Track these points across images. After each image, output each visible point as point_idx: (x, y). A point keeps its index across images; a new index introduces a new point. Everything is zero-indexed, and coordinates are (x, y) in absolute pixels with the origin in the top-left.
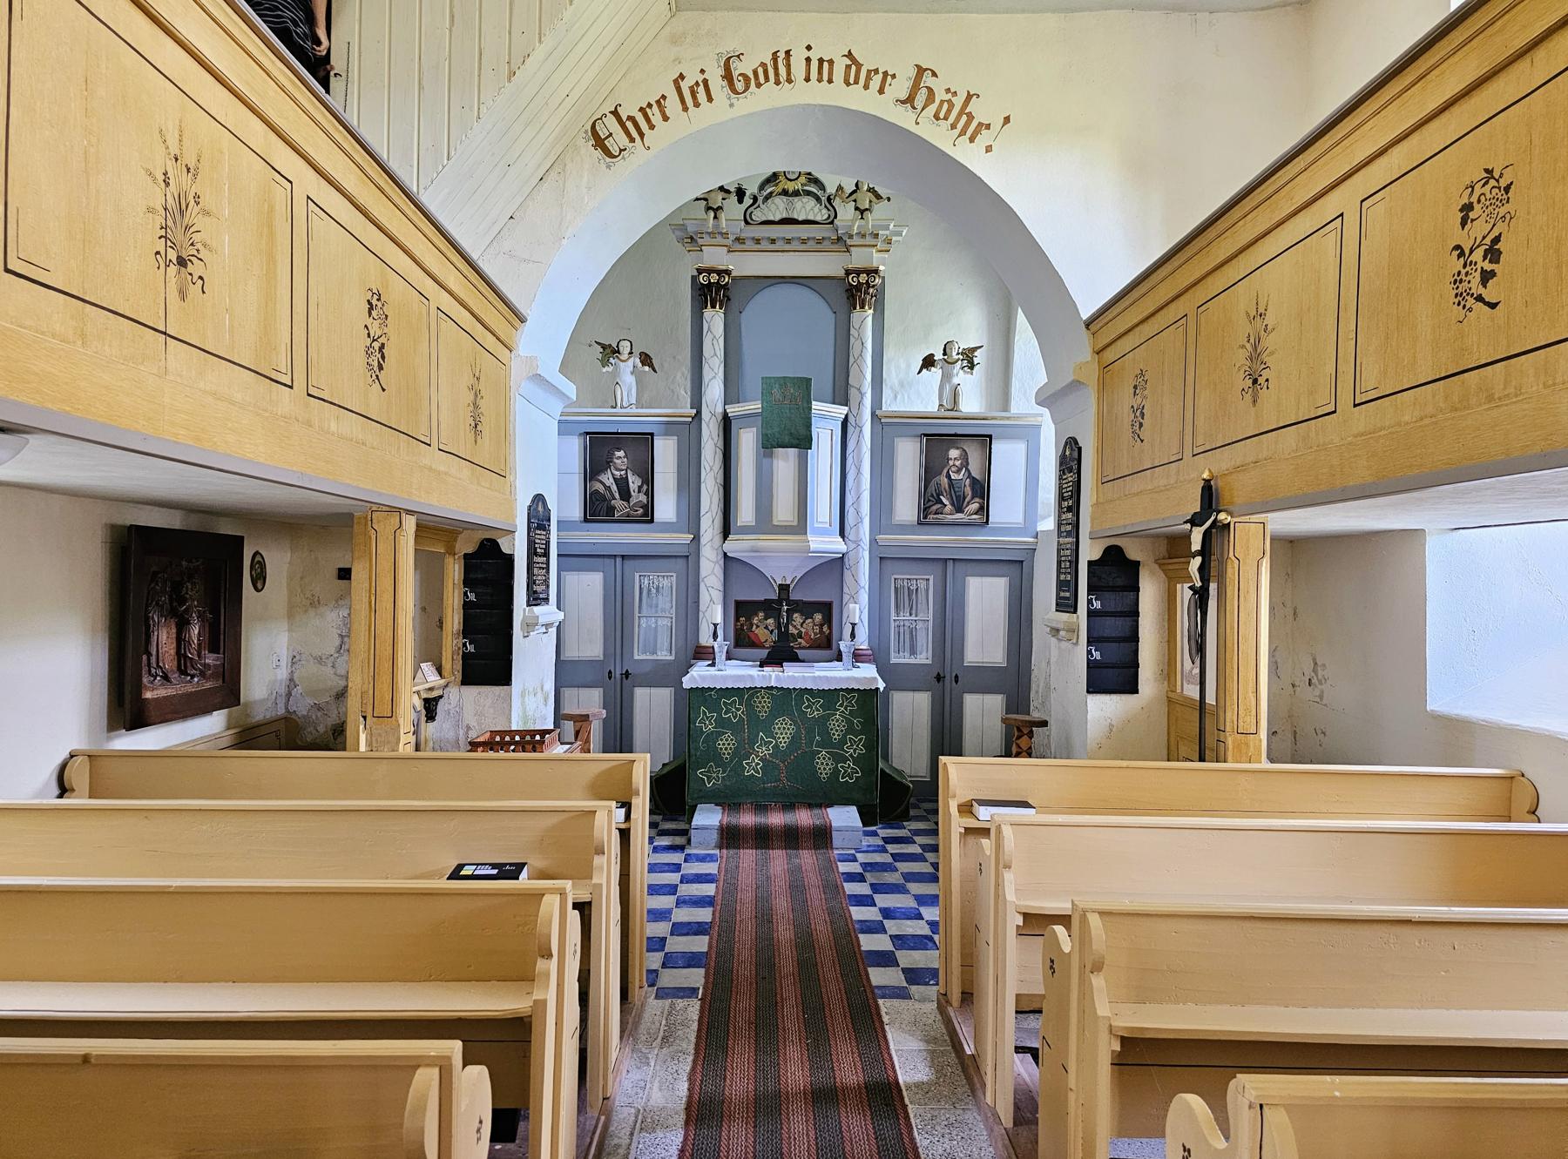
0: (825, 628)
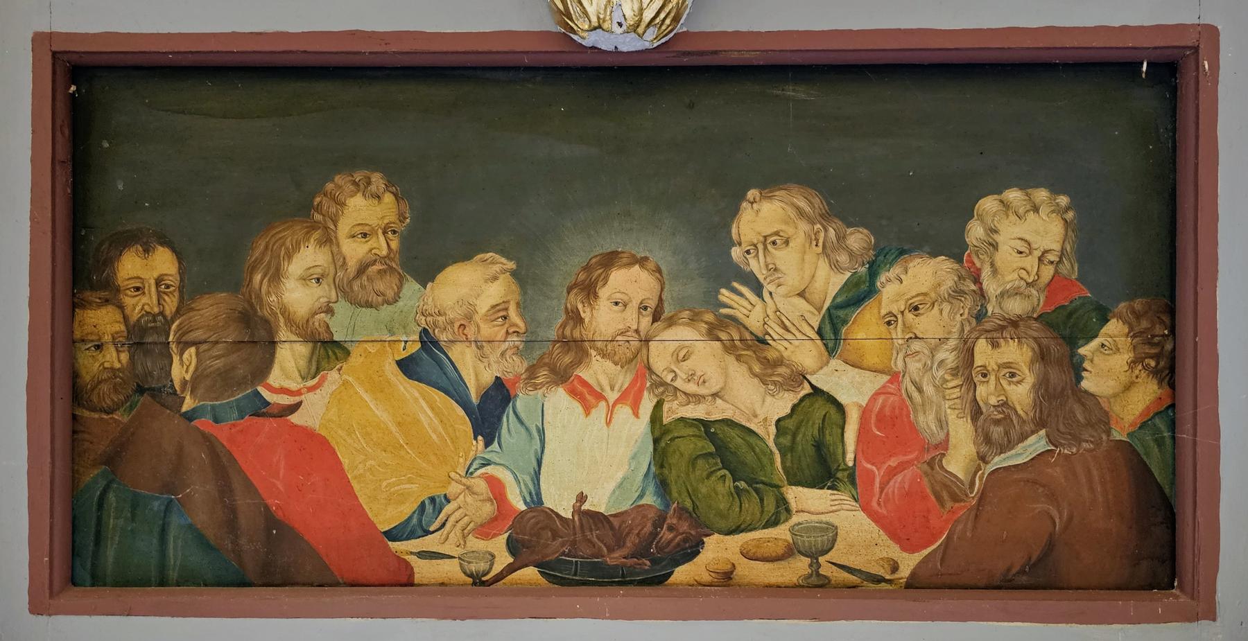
0: (1111, 367)
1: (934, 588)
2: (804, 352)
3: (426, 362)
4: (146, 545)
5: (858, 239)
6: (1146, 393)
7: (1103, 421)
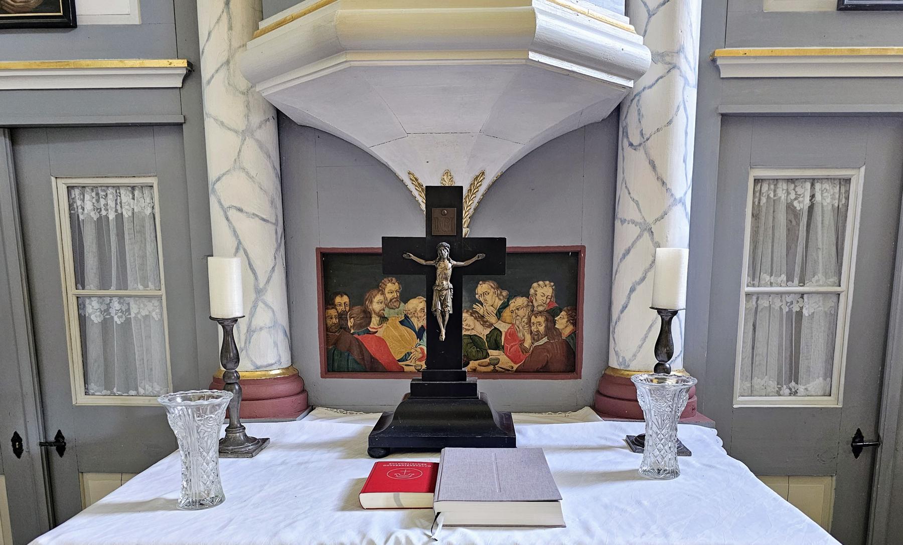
0: (562, 322)
1: (521, 373)
2: (493, 319)
3: (406, 322)
4: (344, 363)
5: (505, 293)
6: (570, 328)
7: (560, 334)
